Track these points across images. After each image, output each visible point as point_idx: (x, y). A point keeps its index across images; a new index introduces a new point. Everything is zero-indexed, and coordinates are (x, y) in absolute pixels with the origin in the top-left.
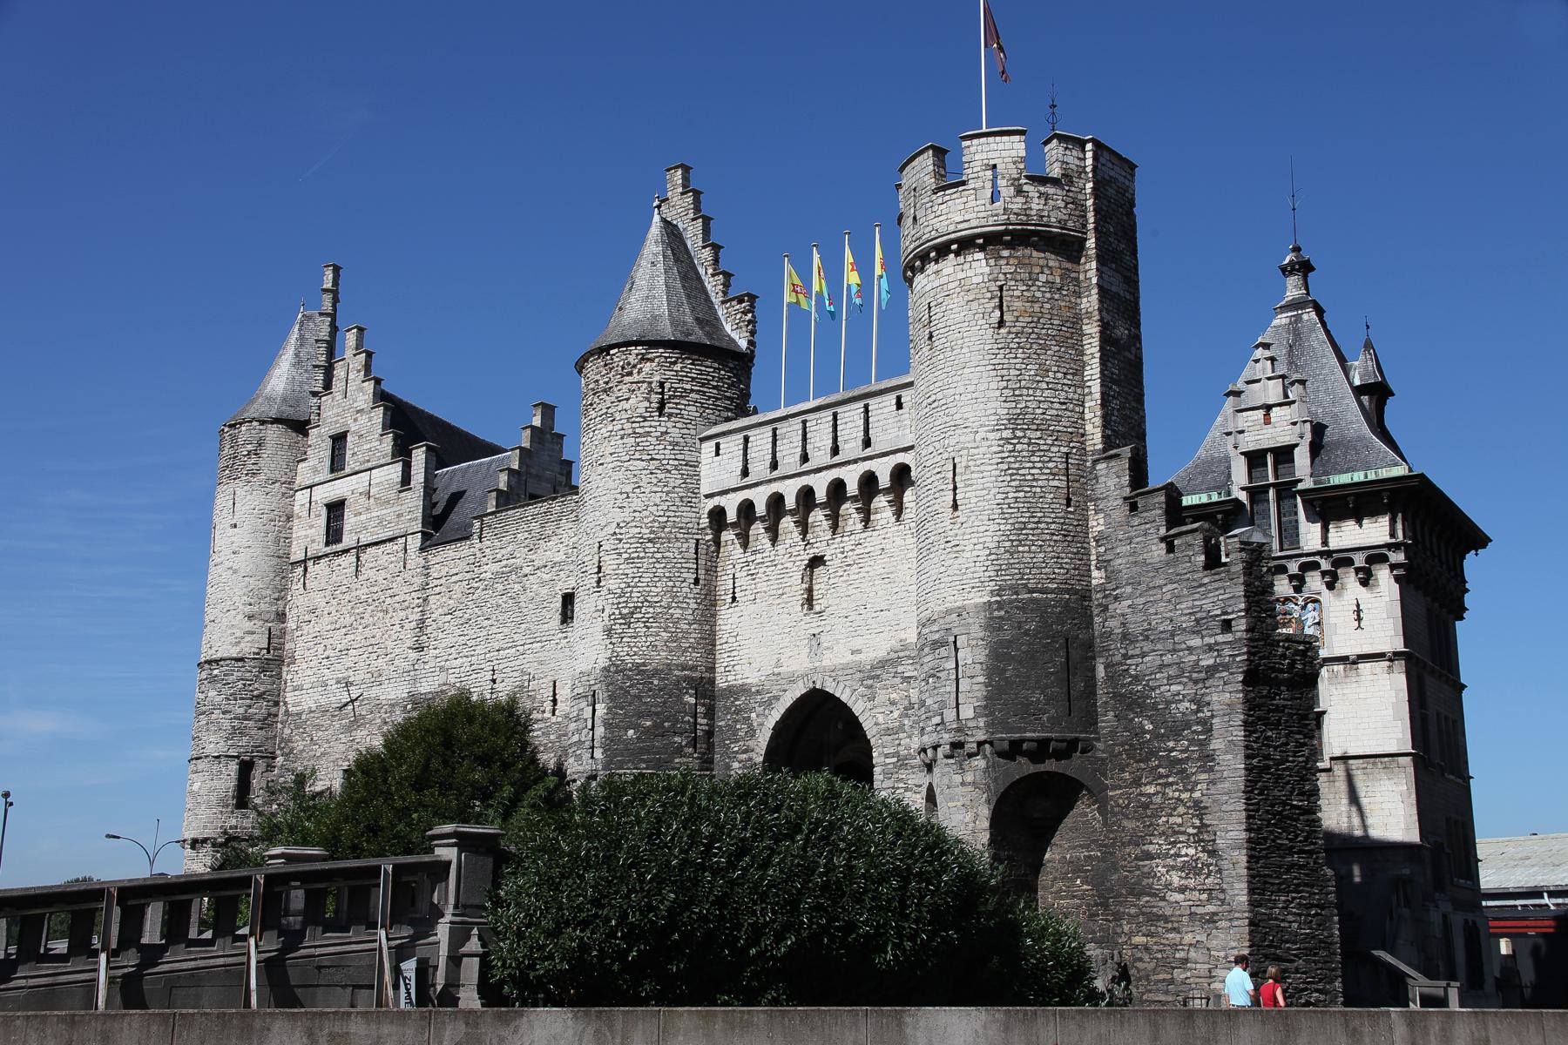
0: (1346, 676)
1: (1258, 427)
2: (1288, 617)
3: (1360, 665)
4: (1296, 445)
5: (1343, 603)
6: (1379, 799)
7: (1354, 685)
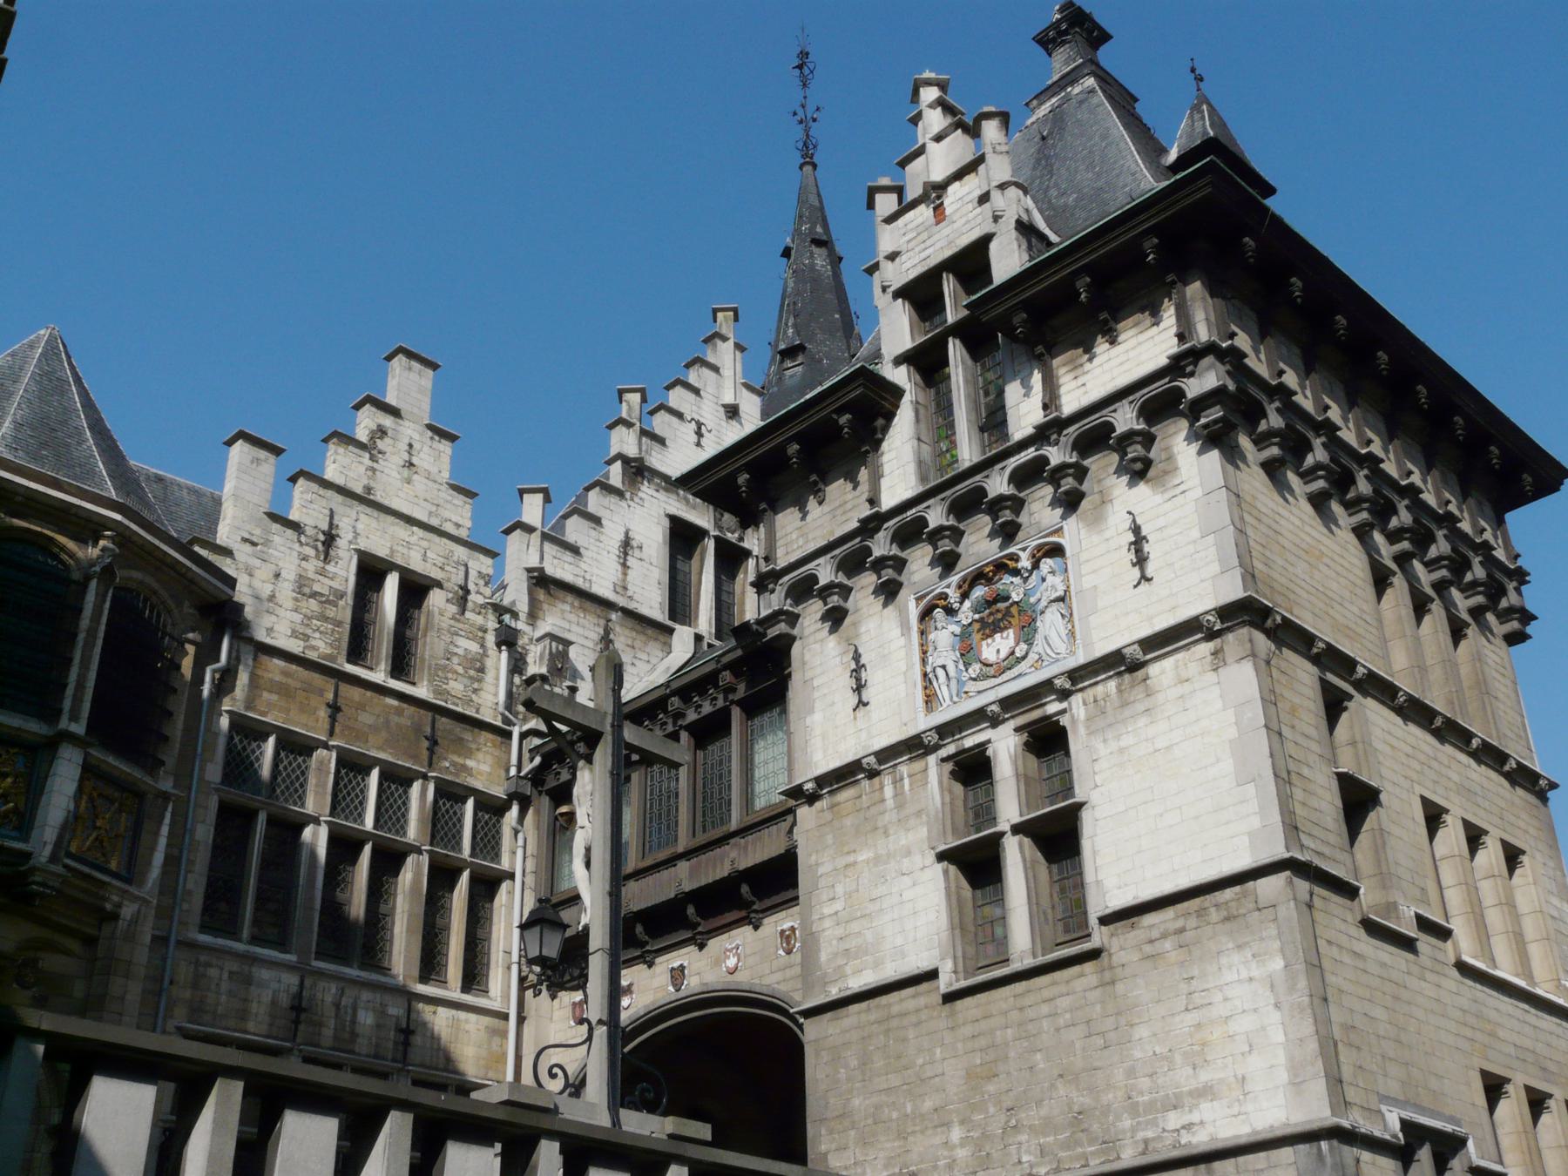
0: (1125, 704)
1: (924, 236)
2: (1001, 606)
3: (1154, 670)
4: (986, 240)
5: (1107, 534)
6: (1220, 1010)
7: (1142, 721)
